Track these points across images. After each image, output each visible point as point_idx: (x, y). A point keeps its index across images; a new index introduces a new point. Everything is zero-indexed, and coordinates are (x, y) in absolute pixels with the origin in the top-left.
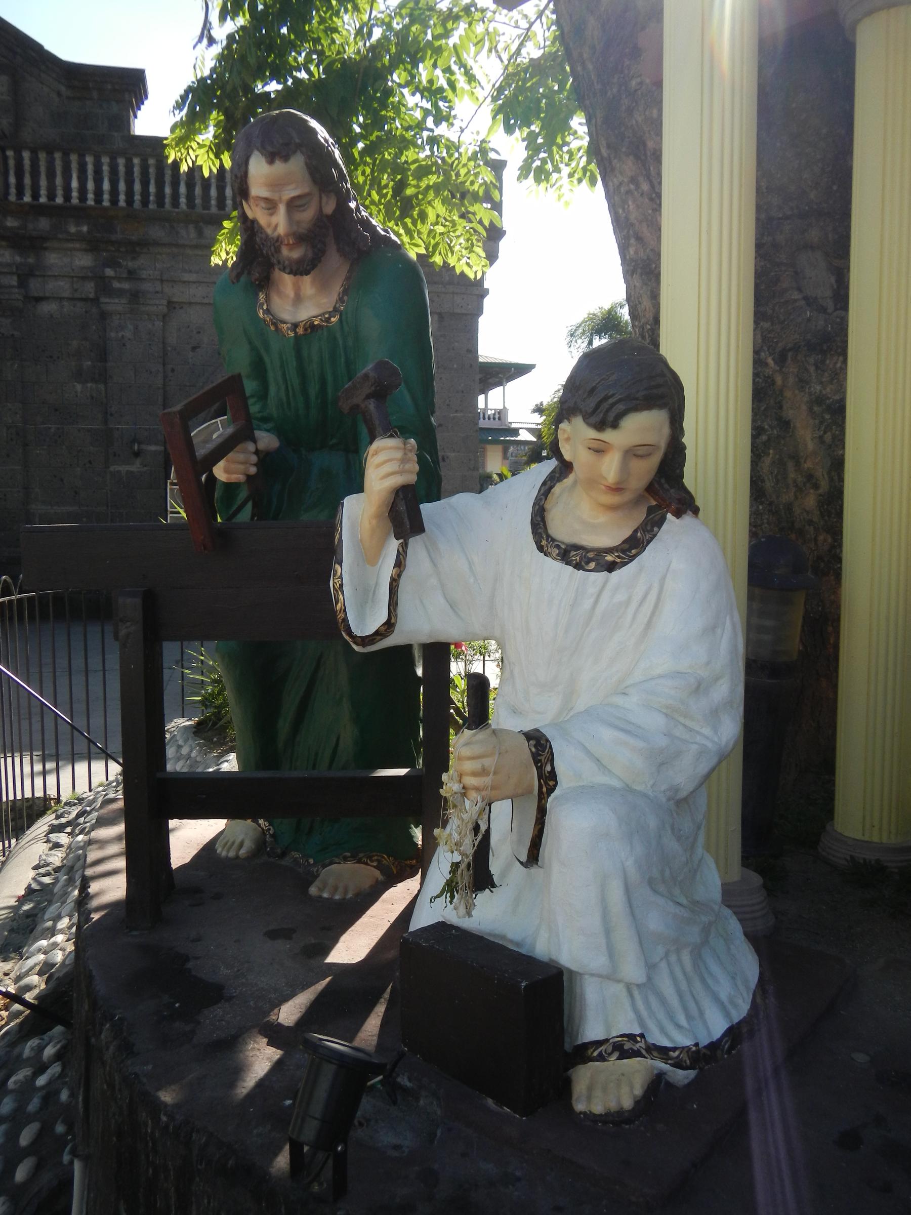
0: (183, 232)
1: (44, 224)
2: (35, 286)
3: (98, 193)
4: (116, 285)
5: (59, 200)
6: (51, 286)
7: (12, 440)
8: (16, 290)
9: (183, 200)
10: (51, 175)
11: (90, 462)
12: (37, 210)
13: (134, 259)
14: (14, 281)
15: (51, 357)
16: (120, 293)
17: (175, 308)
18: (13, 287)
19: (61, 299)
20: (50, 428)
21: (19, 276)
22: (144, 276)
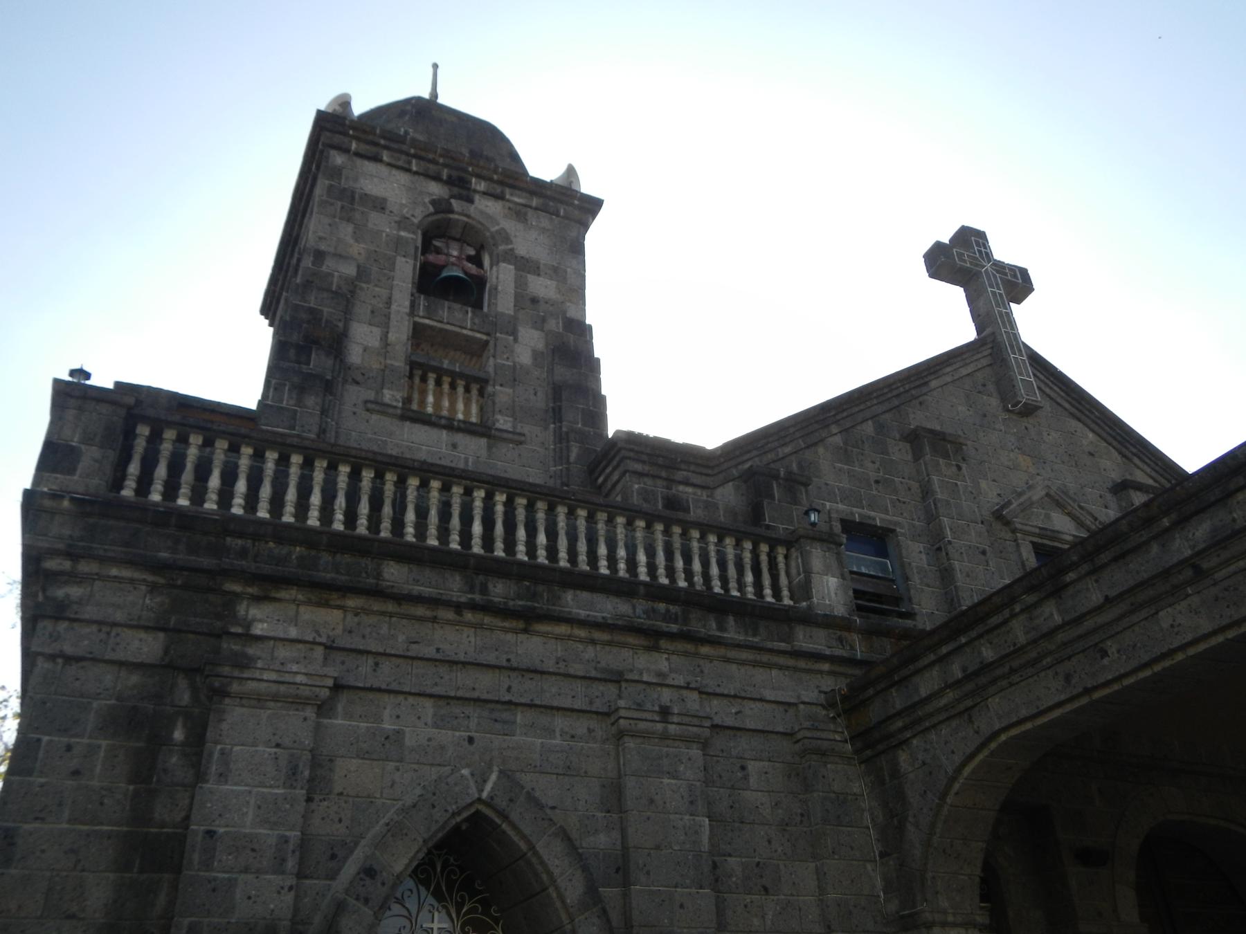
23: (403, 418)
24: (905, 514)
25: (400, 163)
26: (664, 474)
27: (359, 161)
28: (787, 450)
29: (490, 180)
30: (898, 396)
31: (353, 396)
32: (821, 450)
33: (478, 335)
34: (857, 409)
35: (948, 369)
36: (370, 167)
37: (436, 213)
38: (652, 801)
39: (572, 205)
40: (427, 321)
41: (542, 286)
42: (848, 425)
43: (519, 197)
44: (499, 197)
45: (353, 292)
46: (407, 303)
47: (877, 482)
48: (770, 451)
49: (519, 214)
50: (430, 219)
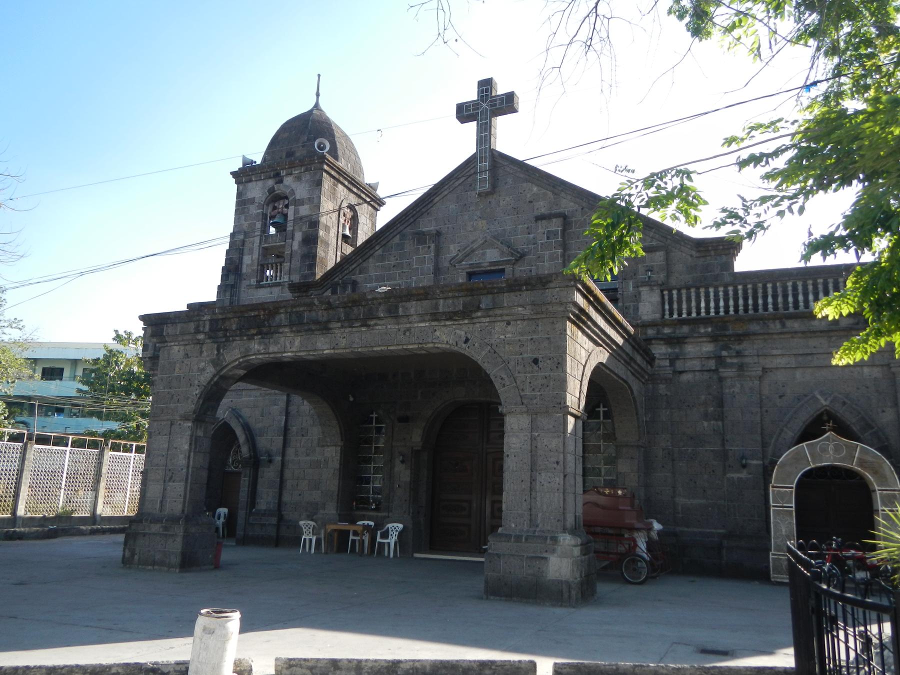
0: (772, 326)
1: (685, 329)
2: (679, 365)
3: (717, 307)
4: (729, 360)
5: (694, 315)
6: (689, 364)
7: (665, 457)
8: (669, 368)
9: (770, 306)
10: (689, 300)
11: (713, 471)
12: (682, 322)
13: (739, 344)
14: (667, 363)
15: (689, 406)
16: (731, 365)
17: (766, 372)
18: (666, 366)
19: (694, 371)
20: (688, 450)
21: (670, 360)
22: (747, 354)
23: (257, 288)
24: (404, 278)
25: (258, 179)
26: (304, 294)
27: (246, 184)
28: (353, 266)
29: (285, 169)
30: (413, 216)
31: (245, 283)
32: (371, 260)
33: (282, 243)
34: (388, 234)
35: (447, 186)
36: (250, 185)
37: (270, 194)
38: (270, 413)
39: (315, 163)
40: (266, 245)
41: (304, 210)
42: (384, 242)
43: (297, 170)
44: (291, 174)
45: (243, 245)
46: (259, 241)
47: (394, 266)
48: (346, 270)
49: (298, 178)
50: (269, 198)
